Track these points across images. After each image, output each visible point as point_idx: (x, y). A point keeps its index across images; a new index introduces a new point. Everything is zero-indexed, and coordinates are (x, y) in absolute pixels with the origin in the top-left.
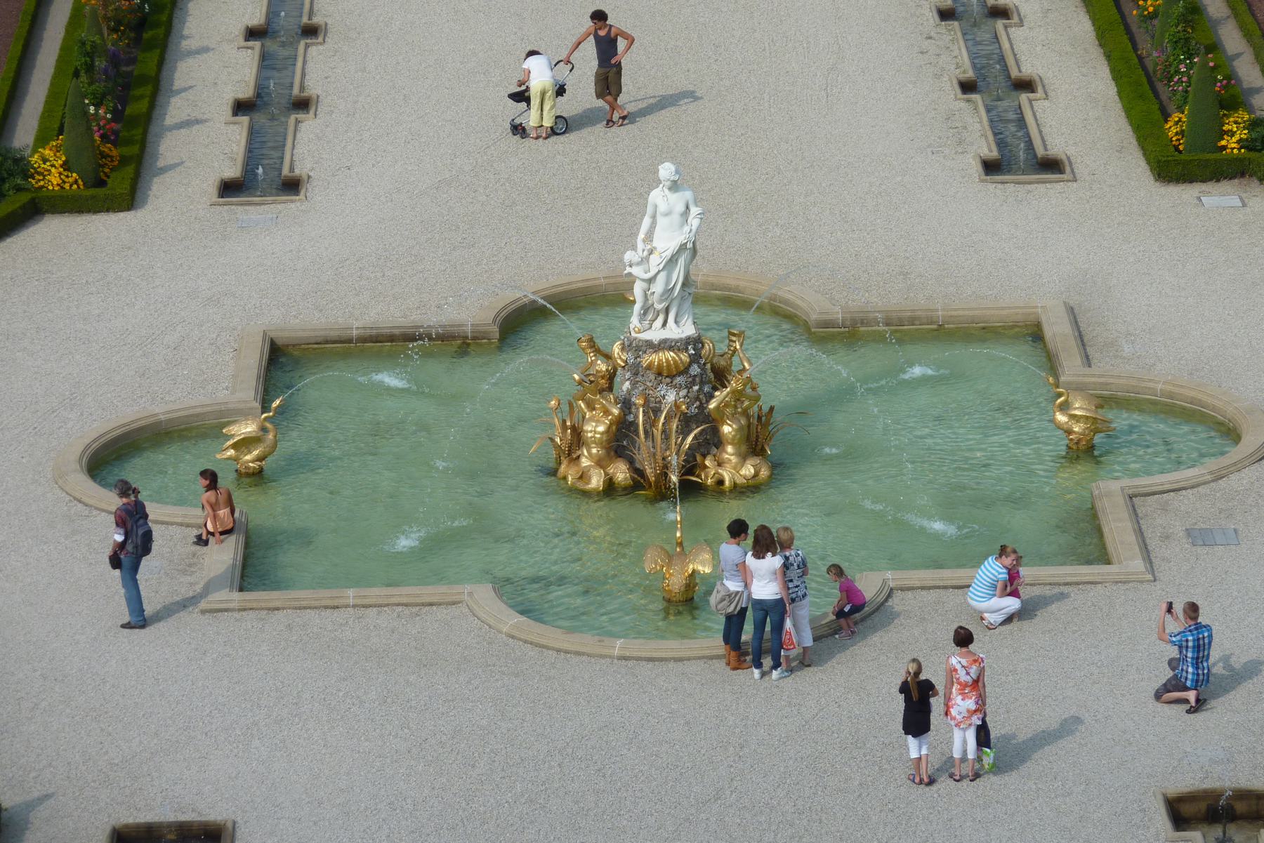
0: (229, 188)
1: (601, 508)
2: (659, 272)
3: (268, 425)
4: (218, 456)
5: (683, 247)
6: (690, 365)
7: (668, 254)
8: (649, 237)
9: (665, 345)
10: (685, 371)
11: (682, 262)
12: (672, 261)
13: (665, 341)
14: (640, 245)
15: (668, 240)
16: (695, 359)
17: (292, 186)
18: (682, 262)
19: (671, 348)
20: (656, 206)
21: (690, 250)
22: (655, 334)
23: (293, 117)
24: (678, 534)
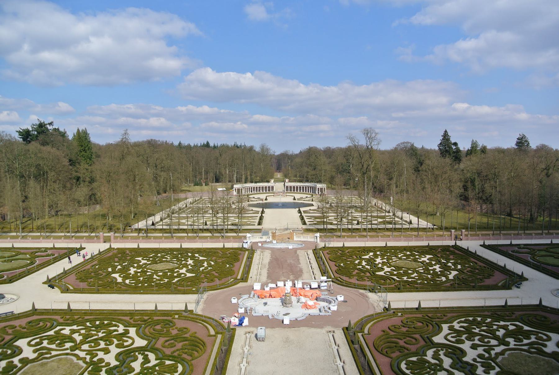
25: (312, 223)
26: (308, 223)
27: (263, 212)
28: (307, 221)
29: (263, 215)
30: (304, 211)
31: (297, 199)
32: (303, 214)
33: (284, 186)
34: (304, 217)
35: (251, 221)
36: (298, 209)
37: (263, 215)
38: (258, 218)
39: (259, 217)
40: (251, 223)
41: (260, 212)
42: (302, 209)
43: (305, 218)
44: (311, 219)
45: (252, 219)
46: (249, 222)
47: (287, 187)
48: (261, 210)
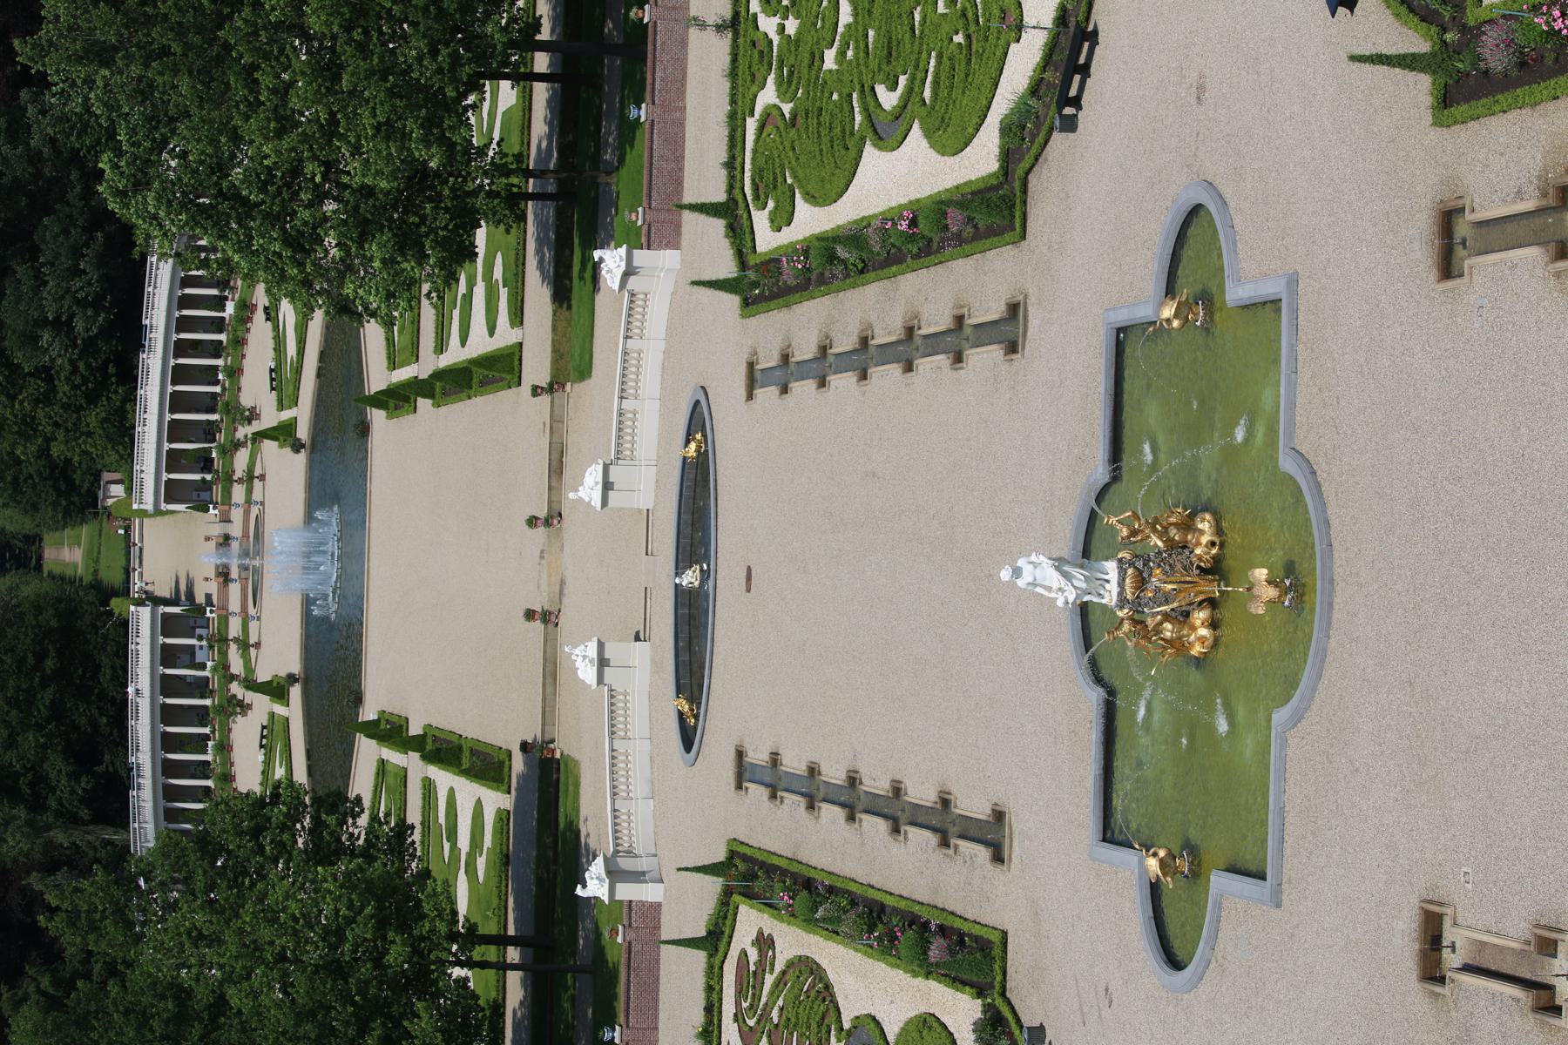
0: (998, 858)
1: (1224, 631)
2: (1072, 585)
3: (1152, 851)
4: (1171, 887)
5: (1057, 568)
6: (1135, 567)
7: (1061, 578)
8: (1049, 589)
9: (1121, 584)
10: (1140, 572)
11: (1066, 568)
12: (1066, 576)
13: (1119, 584)
14: (1053, 595)
15: (1053, 578)
16: (1132, 564)
17: (999, 816)
18: (1066, 568)
19: (1124, 580)
20: (1029, 584)
21: (1059, 563)
22: (1113, 587)
23: (954, 810)
24: (1241, 590)
25: (504, 293)
26: (506, 335)
27: (391, 731)
28: (481, 343)
29: (415, 730)
30: (393, 364)
31: (286, 415)
32: (421, 369)
33: (158, 512)
34: (445, 361)
35: (464, 842)
36: (377, 417)
37: (415, 730)
38: (444, 779)
39: (434, 772)
40: (488, 841)
41: (394, 757)
42: (378, 377)
43: (455, 355)
44: (468, 298)
45: (453, 834)
46: (481, 863)
47: (173, 492)
48: (367, 753)
